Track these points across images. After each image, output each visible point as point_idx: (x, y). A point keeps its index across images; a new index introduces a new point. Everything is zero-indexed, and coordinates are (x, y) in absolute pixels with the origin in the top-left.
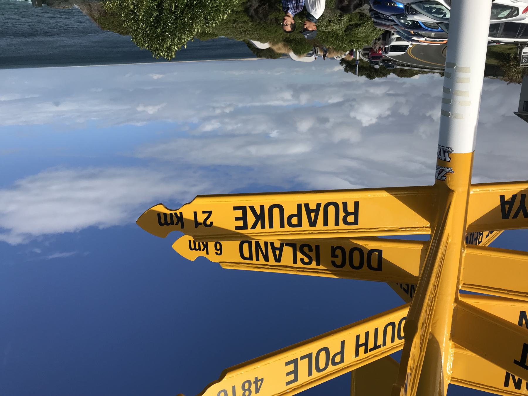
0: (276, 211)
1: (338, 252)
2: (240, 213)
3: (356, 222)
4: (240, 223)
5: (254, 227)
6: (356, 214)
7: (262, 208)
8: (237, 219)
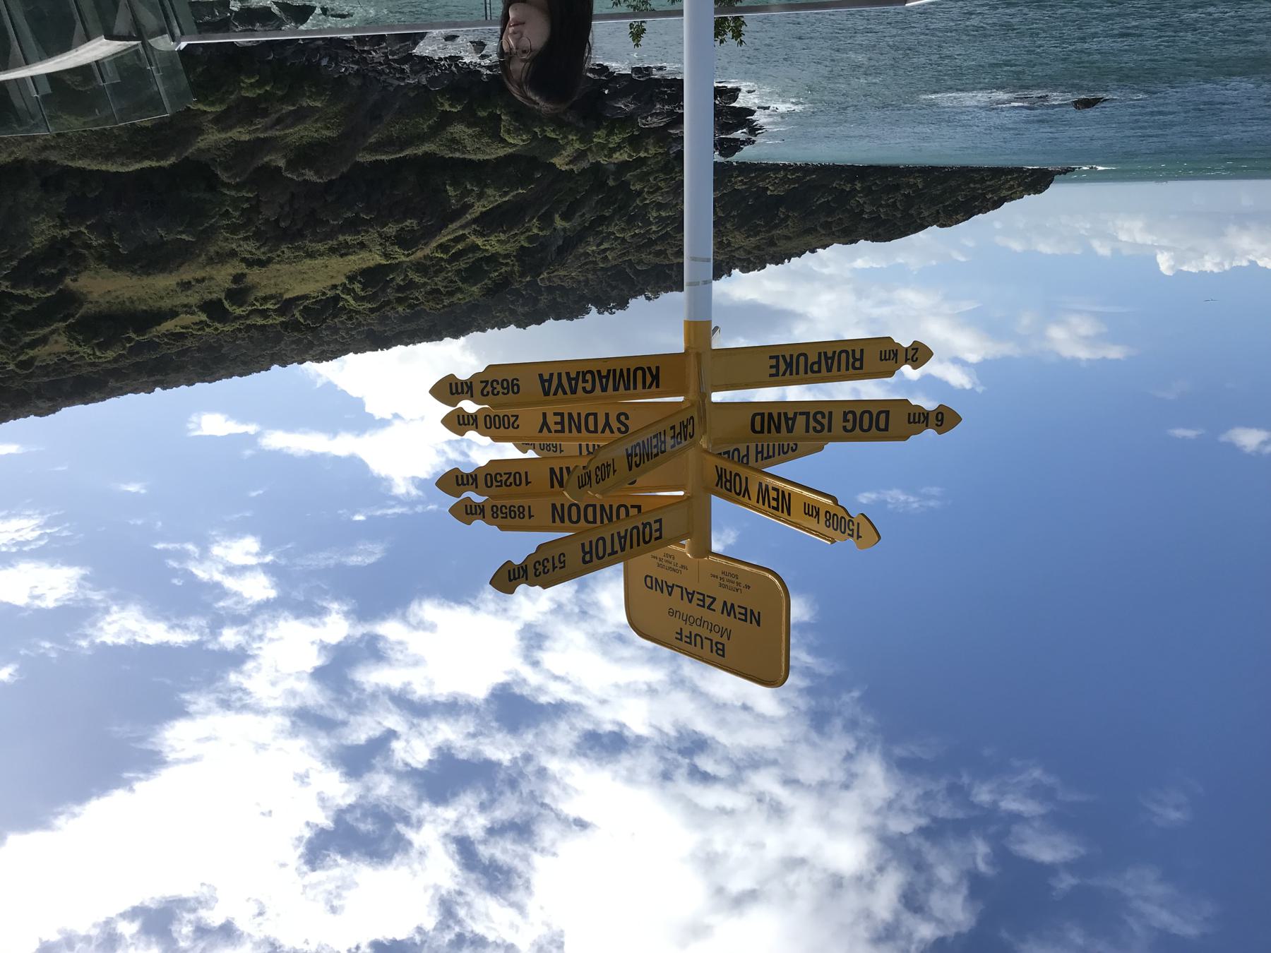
0: (802, 359)
1: (850, 417)
2: (773, 362)
3: (861, 368)
4: (773, 371)
5: (784, 374)
6: (861, 360)
7: (791, 356)
8: (771, 367)
